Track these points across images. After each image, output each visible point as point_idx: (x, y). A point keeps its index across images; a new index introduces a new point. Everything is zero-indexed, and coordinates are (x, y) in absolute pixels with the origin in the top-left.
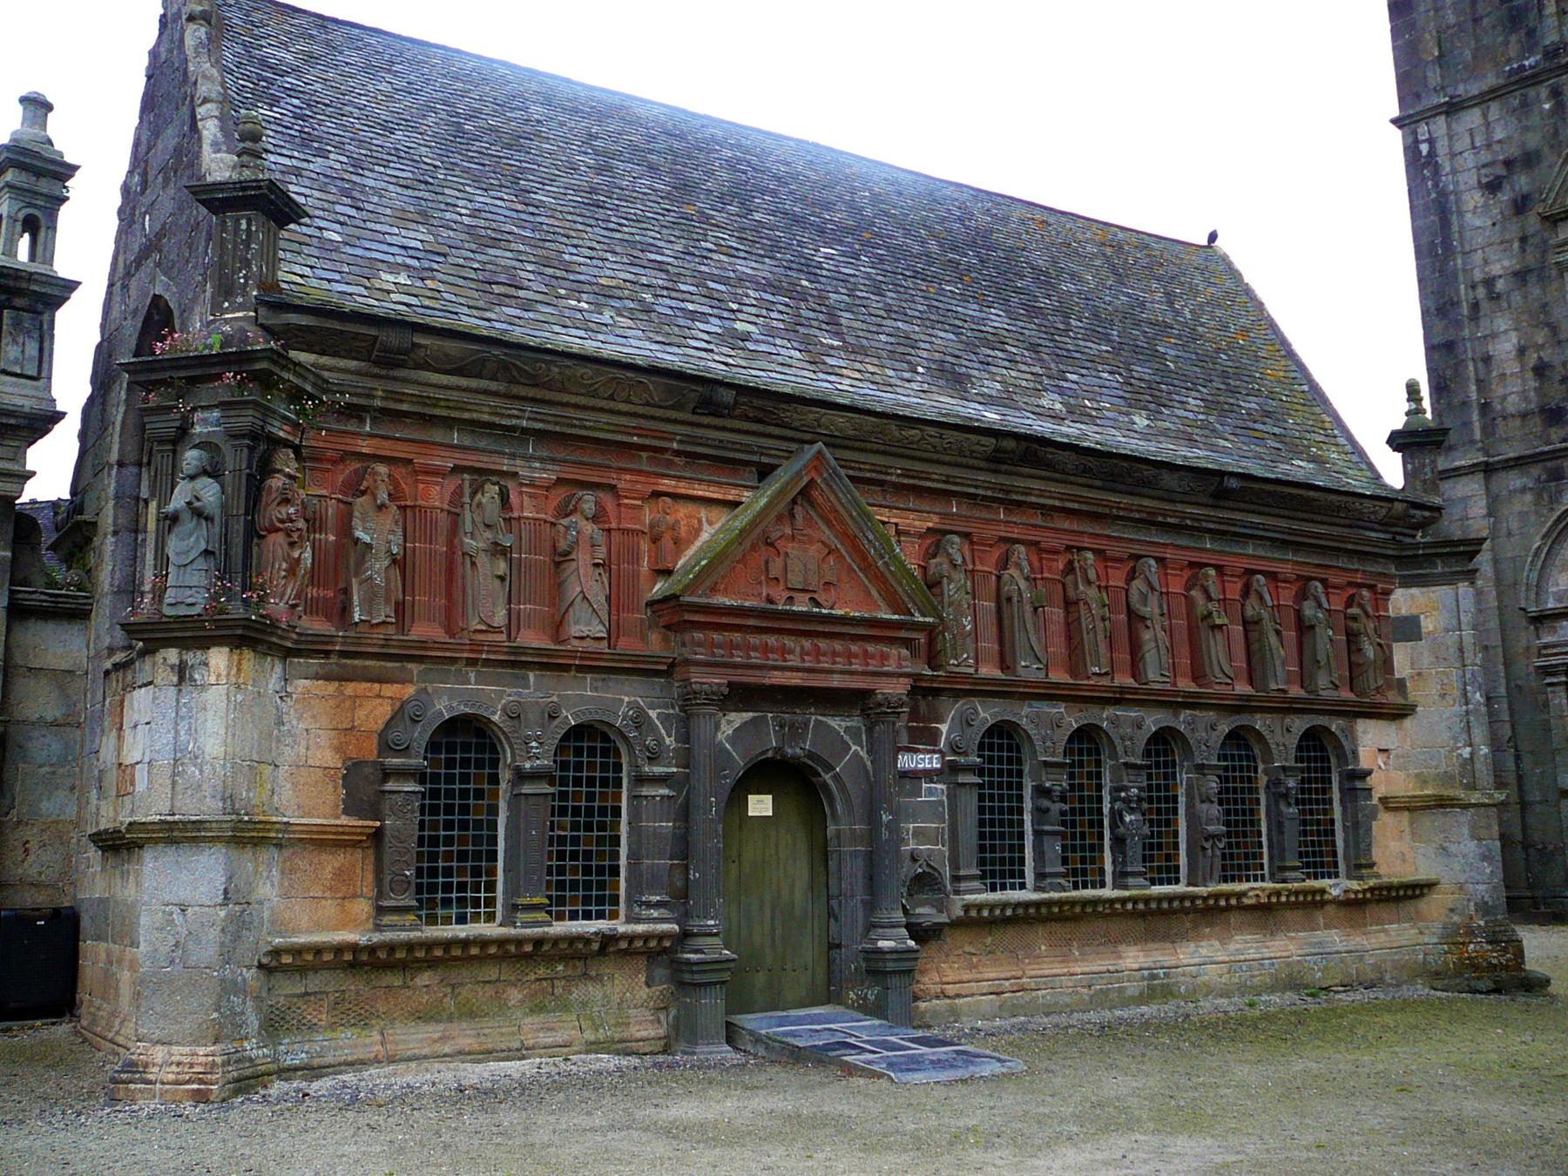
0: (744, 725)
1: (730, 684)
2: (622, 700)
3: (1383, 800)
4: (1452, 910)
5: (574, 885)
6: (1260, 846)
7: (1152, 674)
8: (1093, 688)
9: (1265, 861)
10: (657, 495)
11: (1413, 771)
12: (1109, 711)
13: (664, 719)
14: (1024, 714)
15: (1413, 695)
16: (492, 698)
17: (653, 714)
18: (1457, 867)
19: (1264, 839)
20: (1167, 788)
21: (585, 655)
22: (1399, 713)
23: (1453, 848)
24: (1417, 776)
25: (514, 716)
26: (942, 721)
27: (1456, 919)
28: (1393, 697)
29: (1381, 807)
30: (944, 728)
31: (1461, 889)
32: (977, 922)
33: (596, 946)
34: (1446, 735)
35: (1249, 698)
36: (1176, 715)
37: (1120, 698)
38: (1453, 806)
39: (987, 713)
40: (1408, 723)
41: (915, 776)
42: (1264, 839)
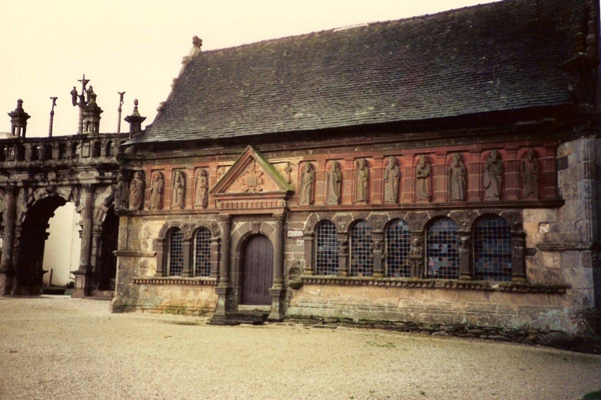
0: (242, 226)
1: (230, 215)
2: (209, 220)
5: (203, 268)
8: (359, 206)
10: (219, 167)
13: (221, 225)
14: (334, 217)
16: (181, 221)
17: (219, 224)
20: (405, 241)
21: (199, 210)
22: (556, 203)
25: (186, 226)
26: (305, 220)
29: (537, 249)
30: (305, 223)
32: (313, 282)
33: (198, 283)
39: (318, 217)
41: (295, 238)
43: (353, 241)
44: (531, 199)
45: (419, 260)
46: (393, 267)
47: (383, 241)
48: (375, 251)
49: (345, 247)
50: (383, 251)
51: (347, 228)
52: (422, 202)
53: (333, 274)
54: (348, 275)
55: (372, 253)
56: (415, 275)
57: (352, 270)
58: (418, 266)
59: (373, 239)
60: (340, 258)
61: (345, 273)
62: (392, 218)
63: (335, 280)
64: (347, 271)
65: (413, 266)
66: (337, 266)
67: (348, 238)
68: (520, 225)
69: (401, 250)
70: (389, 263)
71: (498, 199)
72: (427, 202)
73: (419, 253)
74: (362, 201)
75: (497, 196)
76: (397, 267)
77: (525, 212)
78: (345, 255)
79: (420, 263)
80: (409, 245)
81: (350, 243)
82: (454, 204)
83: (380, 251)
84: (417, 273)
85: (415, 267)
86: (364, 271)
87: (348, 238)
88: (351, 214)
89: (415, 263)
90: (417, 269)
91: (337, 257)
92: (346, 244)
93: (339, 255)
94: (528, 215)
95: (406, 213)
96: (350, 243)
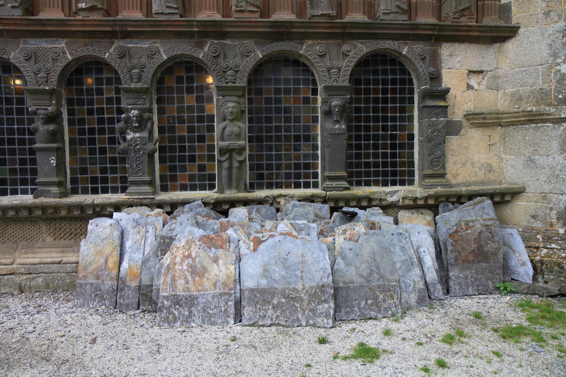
3: (469, 116)
4: (534, 217)
6: (315, 157)
7: (155, 8)
8: (84, 23)
9: (319, 171)
11: (510, 90)
12: (118, 43)
15: (516, 17)
18: (543, 178)
19: (319, 152)
23: (541, 161)
24: (513, 94)
27: (538, 225)
28: (488, 21)
29: (465, 123)
31: (545, 198)
34: (546, 52)
35: (290, 24)
36: (201, 46)
37: (126, 32)
38: (544, 121)
40: (510, 46)
42: (319, 152)
43: (71, 112)
44: (464, 21)
45: (241, 150)
46: (173, 169)
47: (150, 110)
48: (130, 136)
49: (52, 127)
50: (151, 133)
51: (54, 79)
52: (247, 16)
53: (25, 192)
54: (63, 195)
55: (125, 139)
56: (230, 186)
57: (74, 181)
58: (236, 164)
59: (123, 105)
60: (39, 157)
61: (55, 189)
62: (169, 55)
63: (30, 209)
64: (60, 184)
65: (226, 165)
66: (34, 172)
67: (59, 104)
68: (436, 77)
69: (191, 130)
70: (162, 160)
71: (406, 17)
72: (256, 17)
73: (238, 136)
74: (92, 9)
75: (404, 12)
76: (183, 169)
77: (446, 50)
78: (55, 145)
79: (241, 158)
80: (211, 118)
81: (65, 116)
82: (317, 25)
83: (145, 134)
84: (234, 184)
85: (230, 168)
86: (105, 180)
87: (59, 104)
88: (62, 44)
89: (230, 159)
90: (234, 171)
91: (32, 152)
92: (53, 118)
93: (38, 145)
94: (451, 56)
95: (206, 43)
96: (65, 116)
